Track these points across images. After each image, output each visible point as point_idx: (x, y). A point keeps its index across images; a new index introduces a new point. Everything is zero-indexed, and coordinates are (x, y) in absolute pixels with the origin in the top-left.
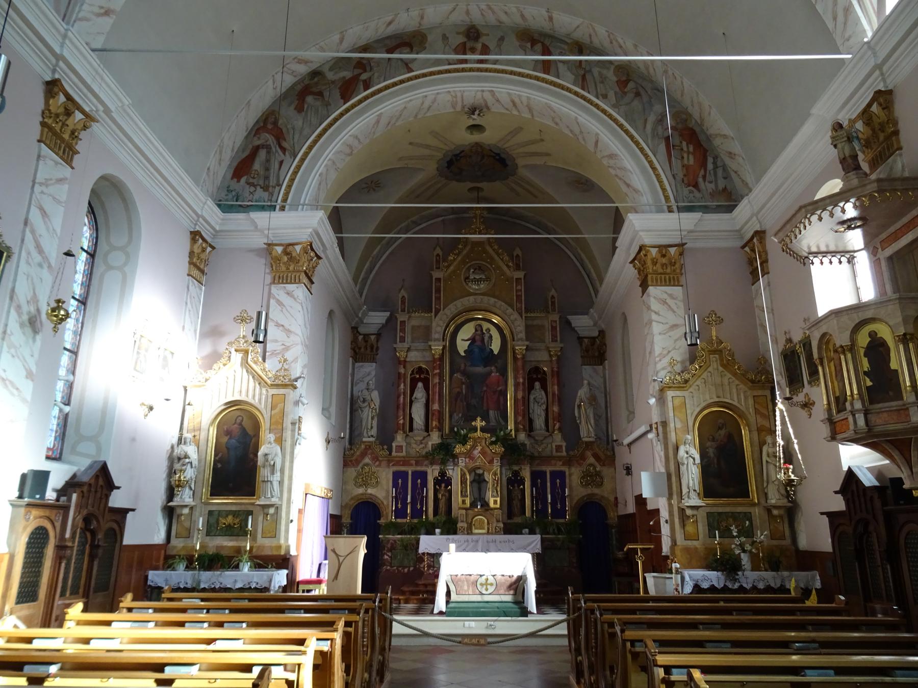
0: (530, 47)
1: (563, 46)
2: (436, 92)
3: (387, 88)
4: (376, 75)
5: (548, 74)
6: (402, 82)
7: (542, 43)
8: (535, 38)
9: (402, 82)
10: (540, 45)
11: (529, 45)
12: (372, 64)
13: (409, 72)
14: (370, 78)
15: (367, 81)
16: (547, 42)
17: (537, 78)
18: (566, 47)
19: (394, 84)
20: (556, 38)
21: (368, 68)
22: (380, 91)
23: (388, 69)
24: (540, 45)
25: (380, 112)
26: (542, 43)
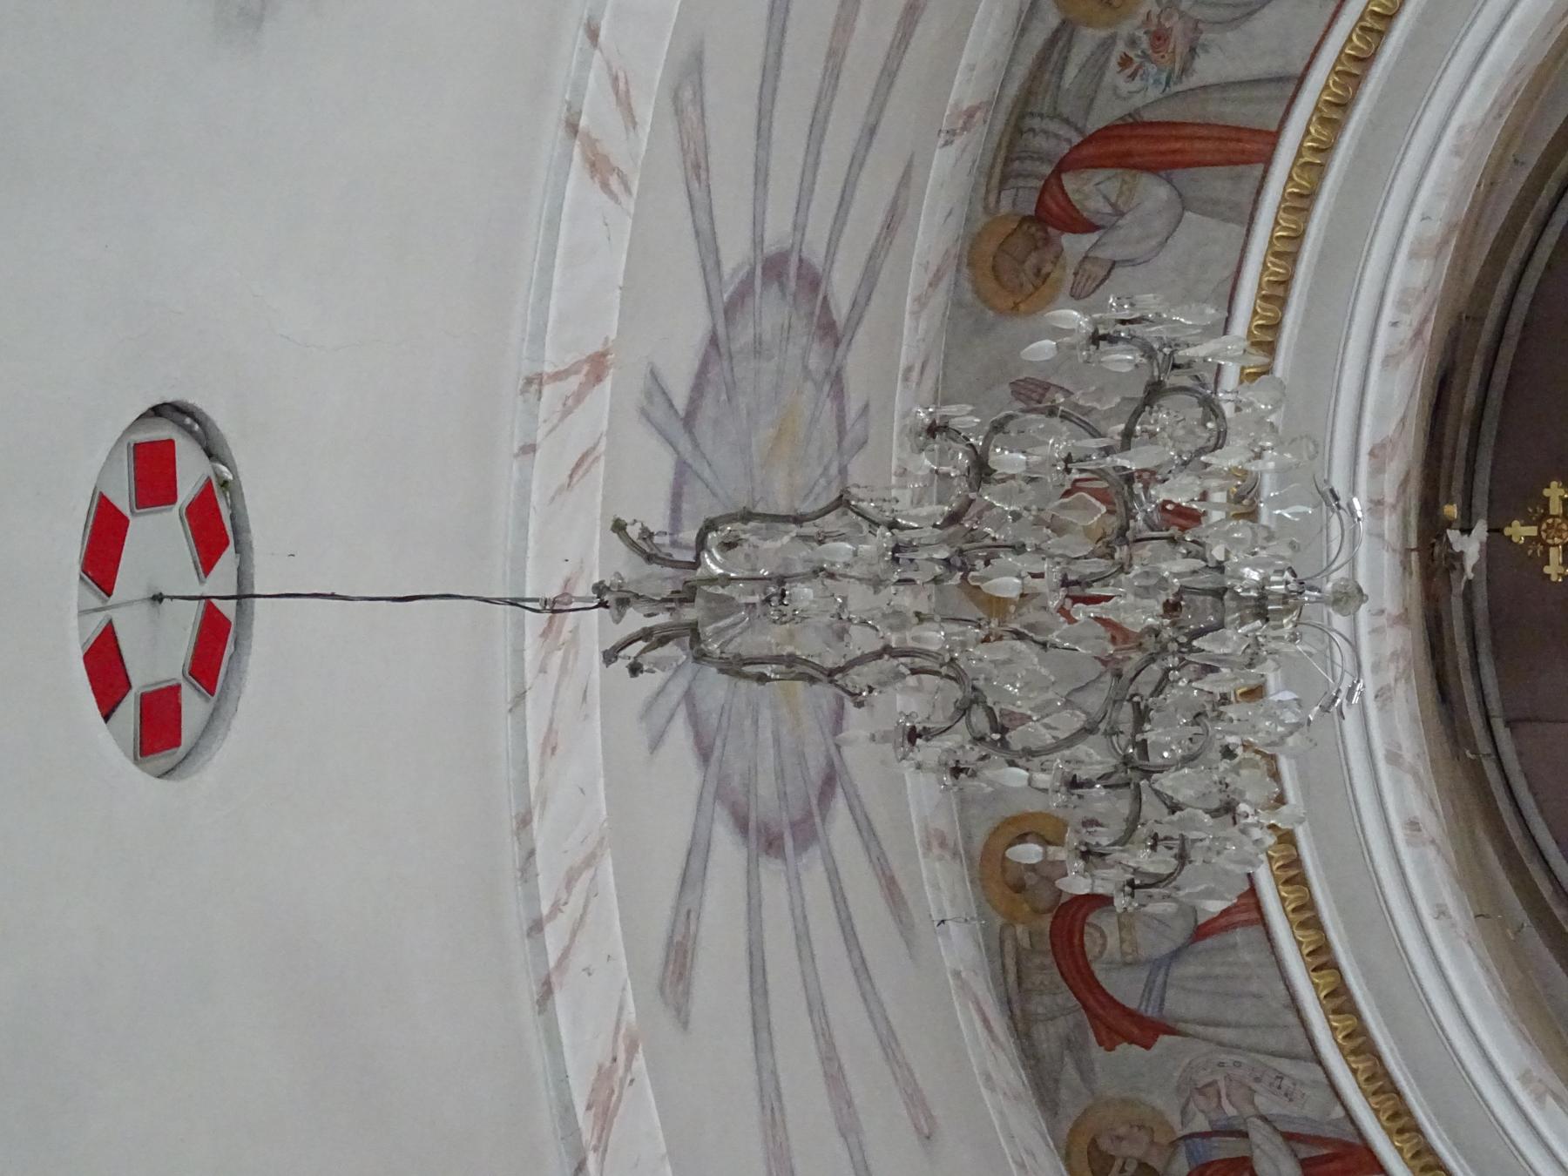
0: (1087, 241)
1: (1081, 52)
2: (1383, 768)
3: (1359, 1044)
4: (1265, 1102)
5: (1273, 138)
6: (1322, 959)
7: (1063, 166)
8: (1030, 210)
9: (1322, 959)
10: (1070, 182)
11: (1074, 245)
12: (1200, 1124)
13: (1262, 920)
14: (1289, 1137)
15: (1305, 1152)
16: (1054, 140)
17: (1300, 202)
18: (1088, 39)
19: (1339, 1000)
20: (1028, 94)
21: (1226, 1149)
22: (1381, 1085)
23: (1227, 1035)
24: (1070, 182)
25: (1515, 1087)
26: (1063, 166)
